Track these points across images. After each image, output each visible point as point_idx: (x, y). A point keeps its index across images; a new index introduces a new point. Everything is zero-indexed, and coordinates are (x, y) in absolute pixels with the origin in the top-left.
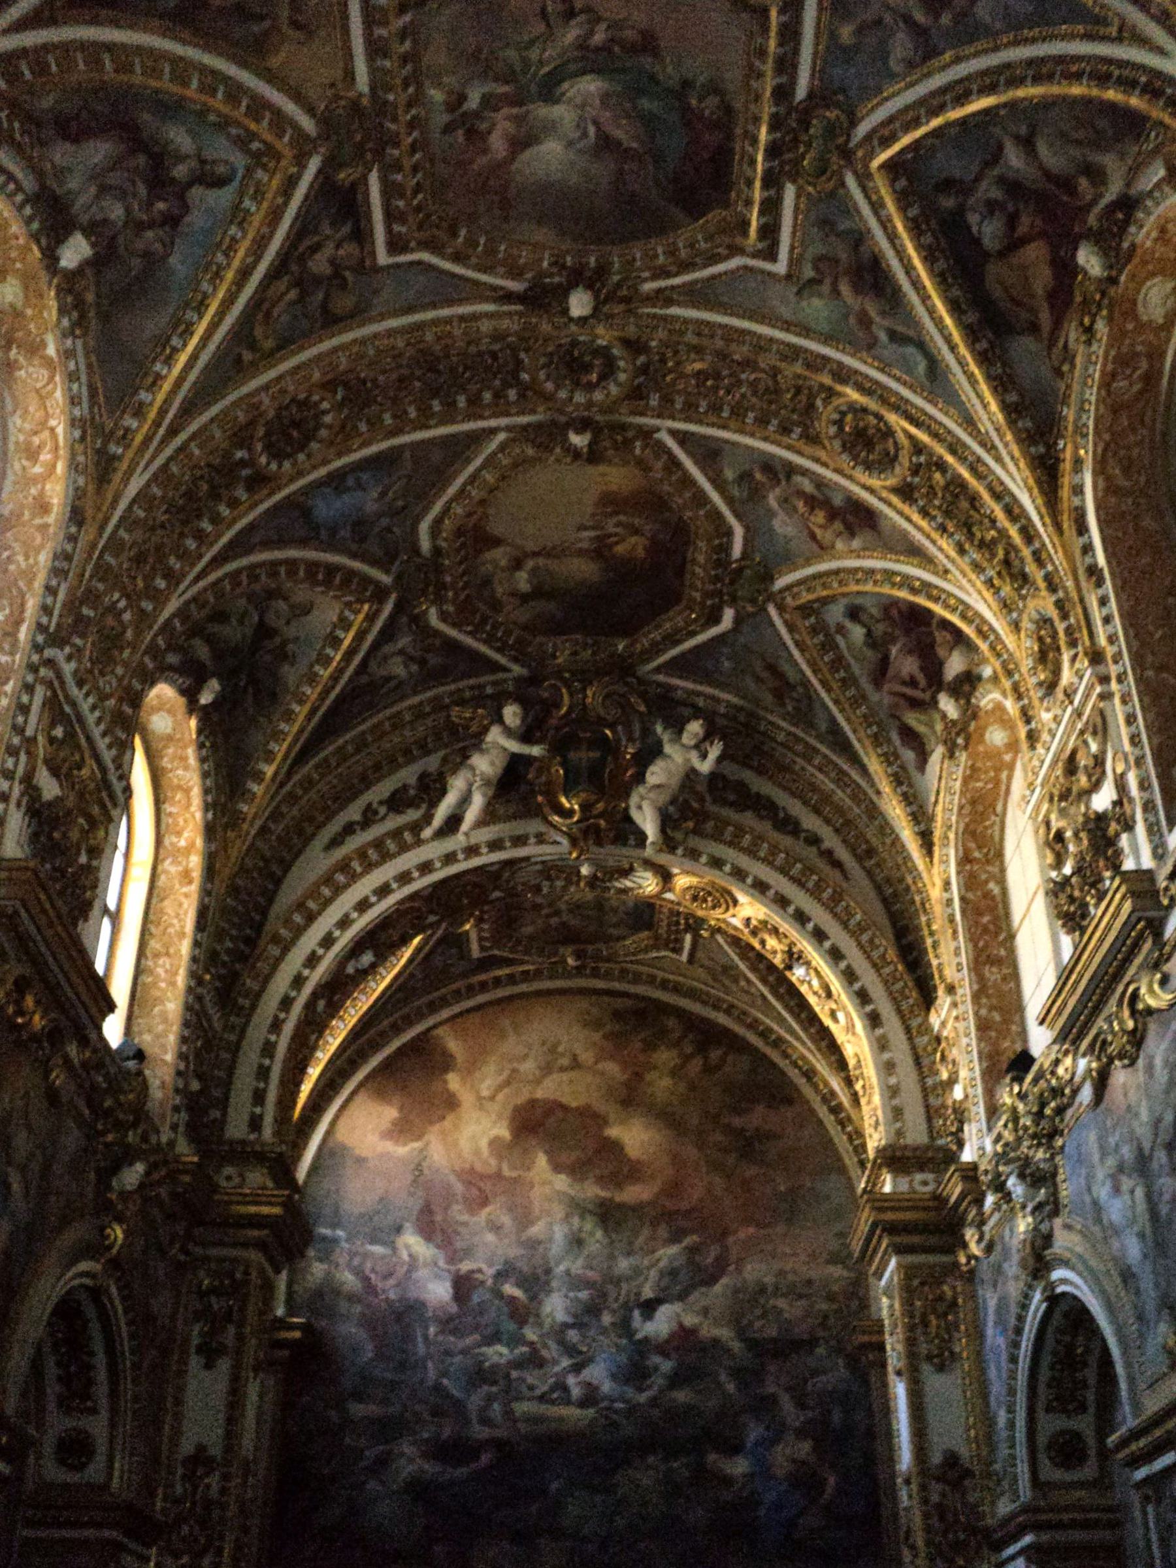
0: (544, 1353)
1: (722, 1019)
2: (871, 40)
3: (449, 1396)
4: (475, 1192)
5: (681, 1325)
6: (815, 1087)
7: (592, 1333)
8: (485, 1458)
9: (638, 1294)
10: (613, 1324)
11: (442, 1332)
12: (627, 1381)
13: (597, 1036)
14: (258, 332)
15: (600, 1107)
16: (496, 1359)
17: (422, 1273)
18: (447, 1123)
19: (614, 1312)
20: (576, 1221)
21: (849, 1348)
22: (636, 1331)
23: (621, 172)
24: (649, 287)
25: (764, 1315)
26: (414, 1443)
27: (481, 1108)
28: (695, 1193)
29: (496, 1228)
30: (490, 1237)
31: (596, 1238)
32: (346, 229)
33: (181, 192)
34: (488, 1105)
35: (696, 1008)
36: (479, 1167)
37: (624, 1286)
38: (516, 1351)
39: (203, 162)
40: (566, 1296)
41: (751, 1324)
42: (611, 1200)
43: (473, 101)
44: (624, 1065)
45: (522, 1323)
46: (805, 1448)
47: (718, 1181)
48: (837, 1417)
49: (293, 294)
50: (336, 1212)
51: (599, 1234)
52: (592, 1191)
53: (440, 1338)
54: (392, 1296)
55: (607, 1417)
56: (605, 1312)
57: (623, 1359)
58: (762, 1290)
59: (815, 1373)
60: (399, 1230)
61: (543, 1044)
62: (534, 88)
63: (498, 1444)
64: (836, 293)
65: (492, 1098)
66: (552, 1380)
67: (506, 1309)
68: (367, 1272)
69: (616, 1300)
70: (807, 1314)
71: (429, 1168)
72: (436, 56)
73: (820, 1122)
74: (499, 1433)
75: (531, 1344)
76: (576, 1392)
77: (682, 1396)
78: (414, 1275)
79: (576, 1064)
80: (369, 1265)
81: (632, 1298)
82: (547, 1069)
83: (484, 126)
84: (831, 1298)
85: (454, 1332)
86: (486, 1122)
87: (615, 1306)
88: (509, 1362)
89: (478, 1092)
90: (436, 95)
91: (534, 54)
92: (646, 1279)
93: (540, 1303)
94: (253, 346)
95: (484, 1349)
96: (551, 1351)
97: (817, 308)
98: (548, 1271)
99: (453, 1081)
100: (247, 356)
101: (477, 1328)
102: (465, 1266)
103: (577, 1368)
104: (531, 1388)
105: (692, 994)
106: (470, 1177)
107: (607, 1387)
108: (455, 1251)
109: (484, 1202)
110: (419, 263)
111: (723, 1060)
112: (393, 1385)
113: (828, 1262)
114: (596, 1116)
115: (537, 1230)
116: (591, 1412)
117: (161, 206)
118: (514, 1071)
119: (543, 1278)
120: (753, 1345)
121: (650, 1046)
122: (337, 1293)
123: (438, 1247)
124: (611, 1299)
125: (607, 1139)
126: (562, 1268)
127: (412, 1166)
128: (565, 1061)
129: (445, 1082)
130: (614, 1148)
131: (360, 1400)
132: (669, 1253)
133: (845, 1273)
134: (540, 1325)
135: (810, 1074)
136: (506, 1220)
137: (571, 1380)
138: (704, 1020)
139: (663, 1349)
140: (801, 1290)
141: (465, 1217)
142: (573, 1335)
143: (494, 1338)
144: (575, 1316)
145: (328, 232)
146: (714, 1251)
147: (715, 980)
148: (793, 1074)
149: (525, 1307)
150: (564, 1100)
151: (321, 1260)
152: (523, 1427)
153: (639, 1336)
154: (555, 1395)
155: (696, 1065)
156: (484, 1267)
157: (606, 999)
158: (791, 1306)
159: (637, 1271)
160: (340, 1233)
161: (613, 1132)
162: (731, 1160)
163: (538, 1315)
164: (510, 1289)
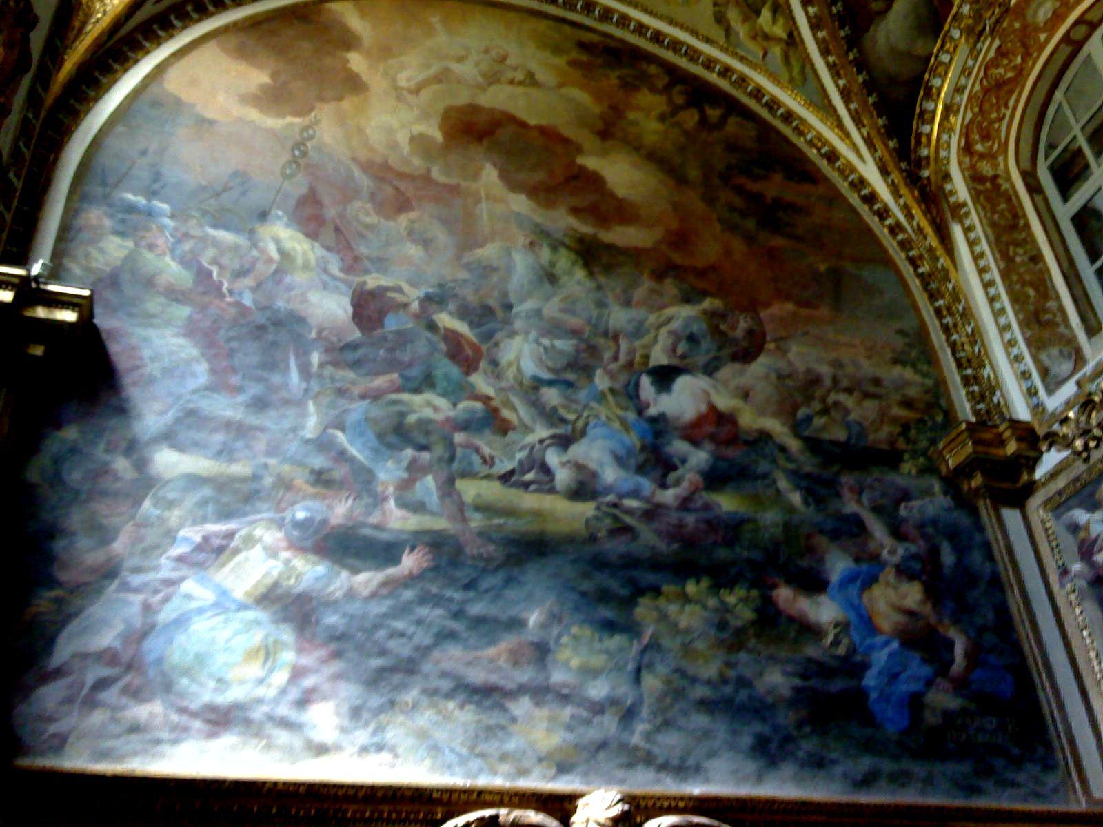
0: (506, 413)
1: (713, 78)
3: (342, 455)
4: (389, 190)
5: (712, 408)
6: (841, 171)
7: (582, 395)
8: (410, 562)
9: (647, 357)
10: (612, 390)
11: (336, 364)
12: (641, 469)
13: (561, 61)
15: (568, 132)
16: (428, 413)
17: (299, 278)
18: (346, 104)
19: (612, 376)
20: (546, 254)
21: (944, 470)
22: (648, 406)
25: (825, 411)
26: (280, 524)
27: (399, 98)
28: (709, 250)
29: (426, 243)
30: (414, 251)
31: (576, 280)
34: (412, 99)
35: (683, 62)
36: (393, 161)
37: (624, 344)
38: (461, 406)
40: (537, 342)
41: (809, 419)
42: (595, 235)
44: (598, 96)
45: (469, 366)
46: (913, 594)
47: (738, 246)
48: (948, 557)
50: (157, 177)
51: (580, 274)
52: (562, 221)
53: (329, 370)
54: (248, 300)
55: (615, 518)
56: (599, 372)
57: (633, 439)
58: (814, 381)
59: (906, 496)
60: (263, 216)
61: (487, 51)
63: (436, 543)
65: (416, 91)
66: (520, 455)
67: (443, 347)
68: (205, 263)
69: (616, 358)
70: (883, 416)
71: (319, 149)
73: (854, 210)
74: (441, 524)
75: (486, 399)
76: (563, 477)
77: (727, 503)
78: (288, 279)
79: (531, 80)
80: (211, 252)
81: (638, 359)
82: (492, 79)
84: (908, 404)
85: (356, 365)
86: (406, 115)
87: (613, 366)
88: (448, 419)
89: (394, 80)
92: (655, 340)
93: (497, 344)
95: (405, 397)
96: (518, 411)
98: (509, 307)
99: (356, 61)
101: (392, 365)
102: (373, 281)
103: (564, 442)
104: (488, 461)
105: (675, 45)
106: (381, 171)
107: (610, 474)
108: (356, 259)
109: (402, 205)
111: (723, 120)
112: (239, 430)
113: (895, 361)
114: (566, 141)
115: (489, 252)
116: (587, 509)
118: (447, 70)
119: (500, 314)
120: (814, 445)
121: (629, 86)
122: (149, 283)
123: (328, 249)
124: (607, 355)
125: (582, 169)
126: (529, 305)
127: (290, 144)
128: (519, 76)
129: (347, 61)
130: (594, 181)
131: (179, 447)
132: (683, 315)
133: (918, 378)
134: (499, 377)
135: (832, 156)
136: (442, 236)
137: (553, 458)
138: (696, 78)
139: (693, 433)
140: (870, 389)
141: (373, 219)
142: (552, 396)
143: (426, 382)
144: (549, 369)
146: (743, 324)
147: (720, 19)
148: (812, 153)
149: (473, 346)
150: (522, 115)
151: (122, 234)
152: (476, 521)
153: (653, 411)
154: (529, 476)
155: (690, 118)
156: (406, 287)
157: (567, 29)
158: (859, 403)
159: (638, 331)
160: (162, 206)
161: (590, 162)
162: (750, 224)
163: (495, 363)
164: (446, 320)
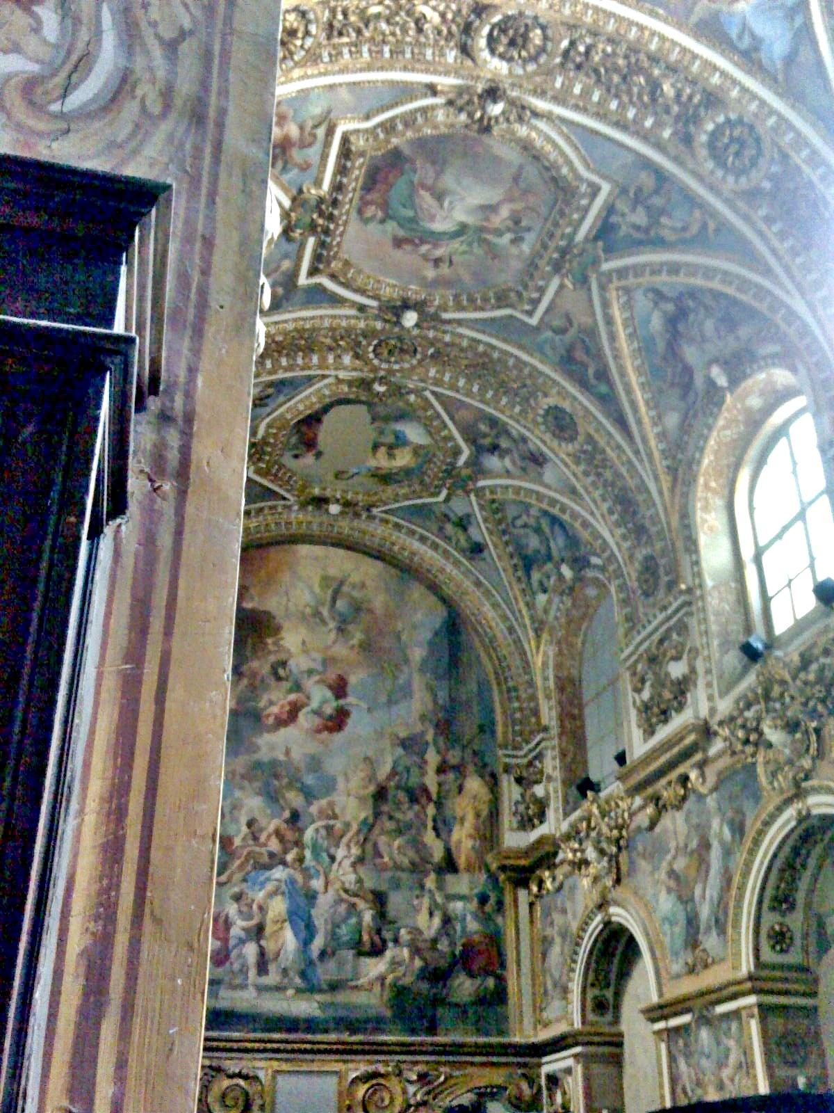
2: (273, 266)
14: (694, 229)
23: (436, 179)
24: (440, 100)
32: (614, 219)
33: (678, 300)
39: (656, 304)
43: (508, 237)
49: (664, 220)
62: (471, 232)
64: (302, 128)
72: (516, 265)
83: (510, 223)
90: (526, 248)
91: (464, 247)
94: (704, 226)
97: (316, 110)
100: (712, 225)
110: (587, 166)
117: (691, 303)
145: (624, 228)
